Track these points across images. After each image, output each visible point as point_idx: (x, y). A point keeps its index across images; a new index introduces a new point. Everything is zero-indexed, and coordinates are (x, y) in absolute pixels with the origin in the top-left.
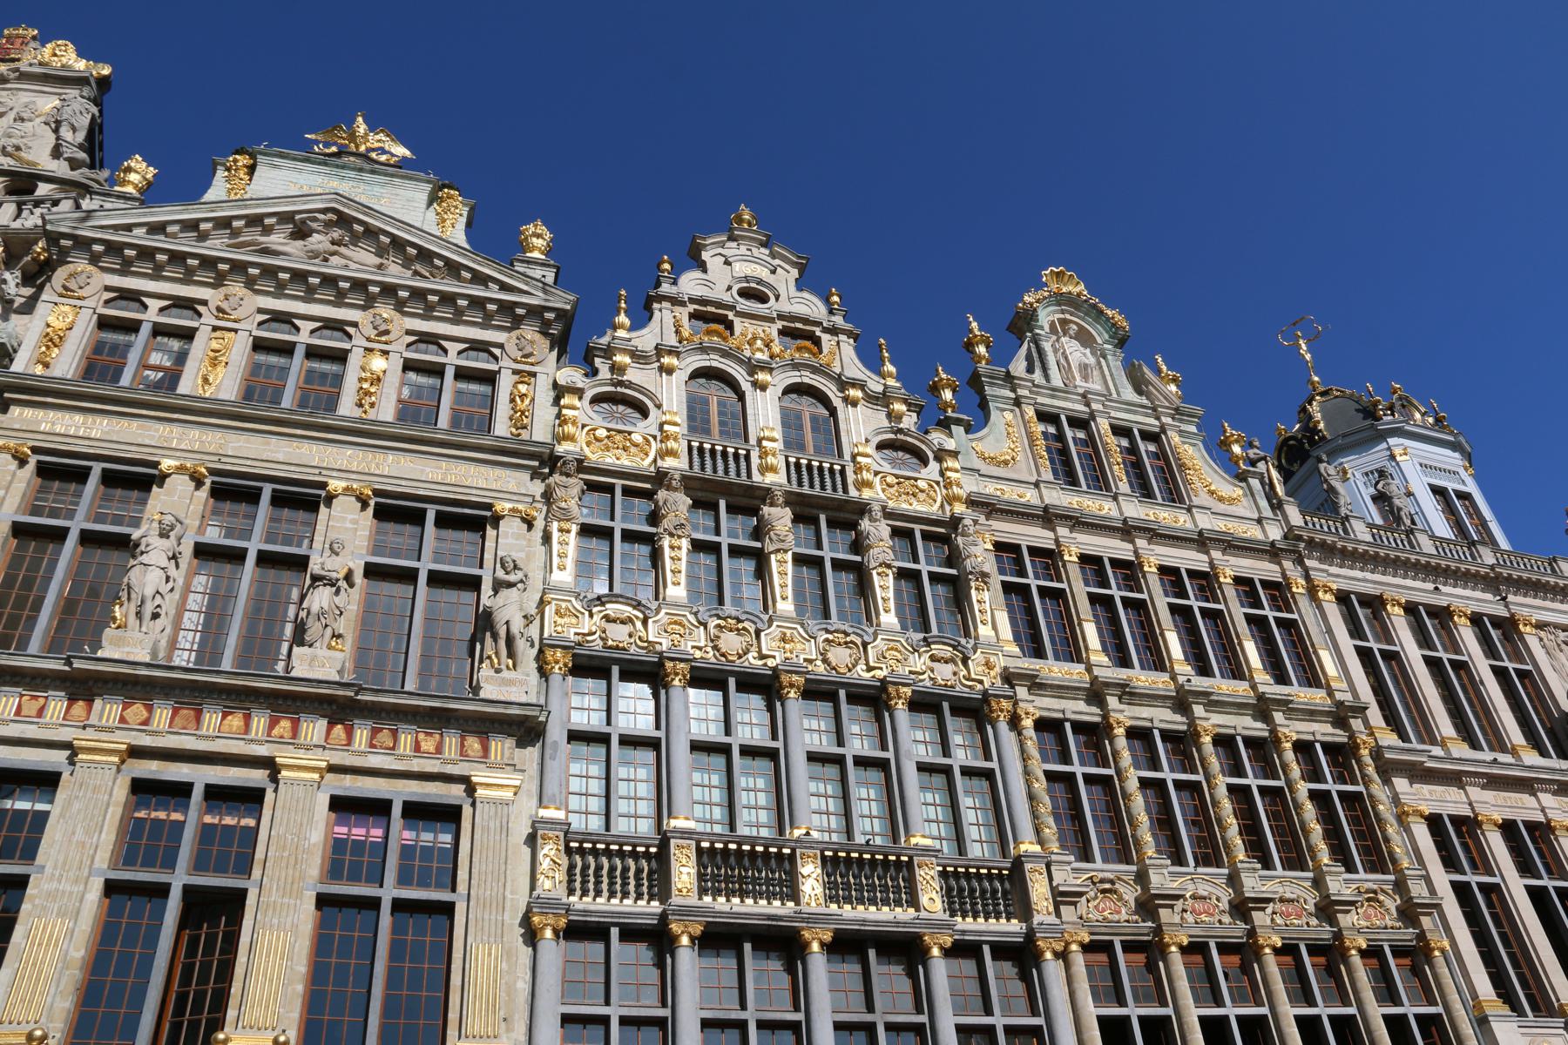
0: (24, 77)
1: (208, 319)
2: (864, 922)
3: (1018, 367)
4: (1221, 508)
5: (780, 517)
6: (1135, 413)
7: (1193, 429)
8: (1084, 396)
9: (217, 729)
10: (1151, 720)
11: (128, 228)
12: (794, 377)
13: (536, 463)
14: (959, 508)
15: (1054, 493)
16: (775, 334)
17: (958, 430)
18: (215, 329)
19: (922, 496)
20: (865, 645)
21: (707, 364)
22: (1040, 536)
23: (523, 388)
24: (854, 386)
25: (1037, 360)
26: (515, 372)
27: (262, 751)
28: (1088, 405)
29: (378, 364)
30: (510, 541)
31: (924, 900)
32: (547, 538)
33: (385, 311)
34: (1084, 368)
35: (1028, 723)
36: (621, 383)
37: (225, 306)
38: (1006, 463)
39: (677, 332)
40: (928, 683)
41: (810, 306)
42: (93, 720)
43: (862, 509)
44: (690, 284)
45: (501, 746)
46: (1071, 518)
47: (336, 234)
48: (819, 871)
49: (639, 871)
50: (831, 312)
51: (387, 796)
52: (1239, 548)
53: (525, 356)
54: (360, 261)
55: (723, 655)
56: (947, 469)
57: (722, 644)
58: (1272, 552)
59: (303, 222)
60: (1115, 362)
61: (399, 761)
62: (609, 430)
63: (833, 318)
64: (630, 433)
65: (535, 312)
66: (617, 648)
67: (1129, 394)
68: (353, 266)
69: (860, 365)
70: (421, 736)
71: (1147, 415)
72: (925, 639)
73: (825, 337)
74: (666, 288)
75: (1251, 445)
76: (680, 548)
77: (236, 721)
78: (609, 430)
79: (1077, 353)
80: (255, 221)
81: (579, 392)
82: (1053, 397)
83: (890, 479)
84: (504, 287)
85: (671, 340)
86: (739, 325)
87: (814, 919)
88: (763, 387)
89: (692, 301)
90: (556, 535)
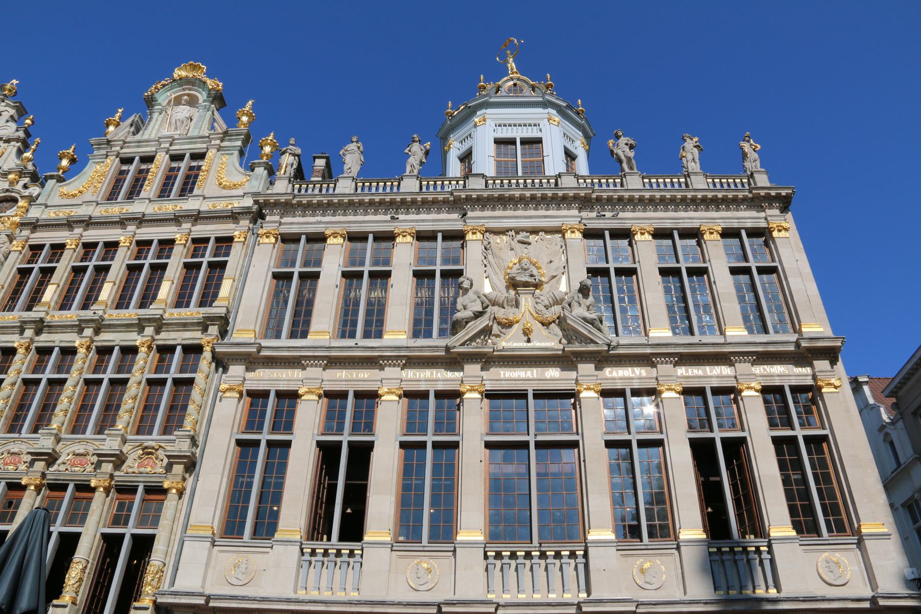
4: (226, 192)
6: (195, 143)
7: (239, 143)
38: (74, 196)
50: (17, 130)
52: (204, 218)
58: (234, 216)
71: (204, 142)
82: (138, 147)
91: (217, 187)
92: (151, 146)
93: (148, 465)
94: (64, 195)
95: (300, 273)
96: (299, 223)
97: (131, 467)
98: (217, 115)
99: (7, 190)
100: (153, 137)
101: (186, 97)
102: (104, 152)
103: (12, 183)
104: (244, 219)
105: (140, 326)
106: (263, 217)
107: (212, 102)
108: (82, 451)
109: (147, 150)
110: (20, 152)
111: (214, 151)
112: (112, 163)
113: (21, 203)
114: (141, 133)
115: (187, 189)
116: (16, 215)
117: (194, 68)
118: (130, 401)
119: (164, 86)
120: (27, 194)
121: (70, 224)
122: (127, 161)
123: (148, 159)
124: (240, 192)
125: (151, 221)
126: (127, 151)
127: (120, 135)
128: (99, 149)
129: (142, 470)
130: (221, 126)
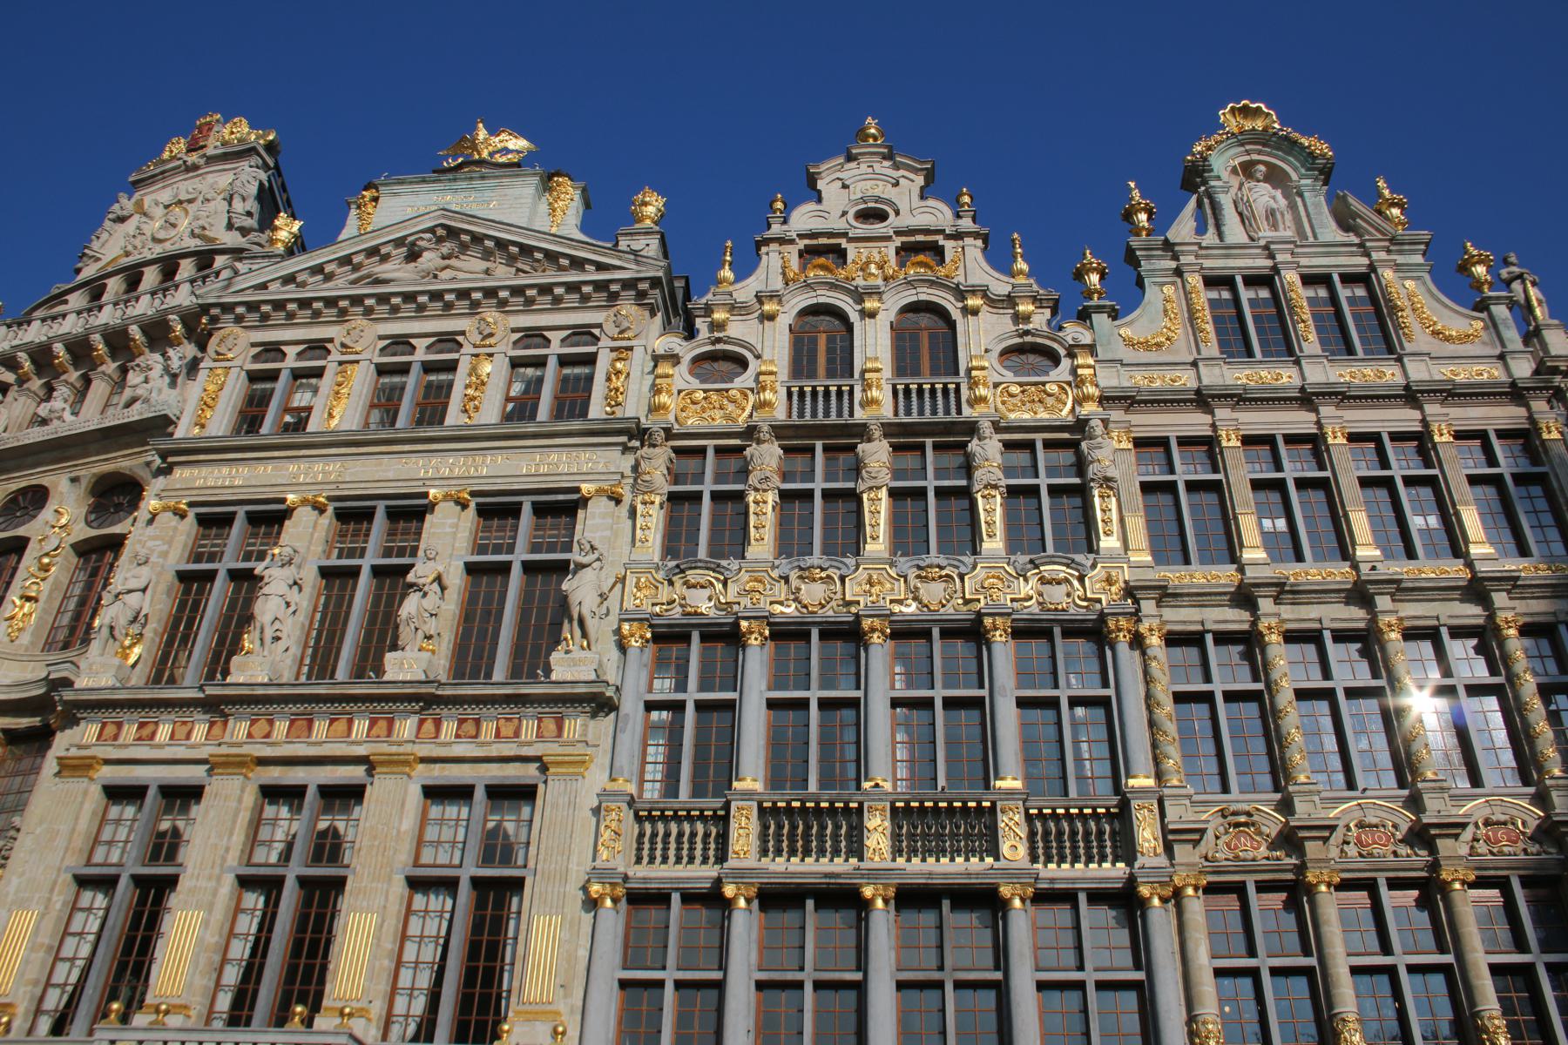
0: (211, 160)
1: (335, 356)
3: (1183, 229)
4: (1450, 349)
5: (877, 454)
6: (1337, 254)
8: (1266, 247)
9: (322, 736)
10: (1320, 621)
12: (909, 297)
13: (624, 439)
14: (1089, 409)
15: (1216, 370)
16: (892, 252)
17: (1100, 320)
18: (341, 363)
19: (1050, 401)
20: (962, 577)
21: (814, 301)
22: (1195, 422)
23: (619, 365)
24: (973, 292)
25: (1210, 215)
26: (613, 350)
27: (361, 751)
28: (1272, 256)
29: (486, 368)
30: (597, 521)
31: (1005, 848)
32: (633, 513)
33: (491, 315)
34: (1271, 214)
35: (1154, 641)
36: (719, 340)
37: (347, 341)
38: (1159, 345)
39: (784, 274)
40: (1036, 609)
41: (937, 214)
42: (227, 739)
43: (971, 428)
44: (804, 218)
45: (576, 725)
46: (1232, 396)
47: (446, 248)
48: (887, 824)
49: (707, 835)
50: (958, 216)
51: (470, 782)
52: (1459, 395)
53: (621, 332)
55: (805, 607)
56: (1078, 366)
57: (803, 596)
59: (413, 244)
60: (1316, 200)
61: (475, 747)
62: (705, 391)
63: (960, 222)
64: (727, 390)
65: (628, 284)
66: (696, 613)
67: (1330, 231)
68: (461, 275)
69: (988, 268)
70: (502, 722)
71: (1352, 254)
72: (1031, 561)
73: (949, 245)
74: (776, 229)
75: (1506, 263)
76: (765, 502)
77: (341, 726)
78: (705, 391)
79: (1264, 196)
80: (373, 252)
81: (674, 359)
82: (1227, 256)
83: (1015, 389)
84: (600, 267)
85: (777, 284)
86: (852, 251)
88: (872, 315)
89: (801, 236)
90: (640, 507)
91: (1431, 339)
94: (1130, 343)
101: (1262, 168)
102: (1173, 264)
103: (1027, 318)
108: (1503, 818)
125: (1360, 397)
126: (1216, 264)
128: (1149, 258)
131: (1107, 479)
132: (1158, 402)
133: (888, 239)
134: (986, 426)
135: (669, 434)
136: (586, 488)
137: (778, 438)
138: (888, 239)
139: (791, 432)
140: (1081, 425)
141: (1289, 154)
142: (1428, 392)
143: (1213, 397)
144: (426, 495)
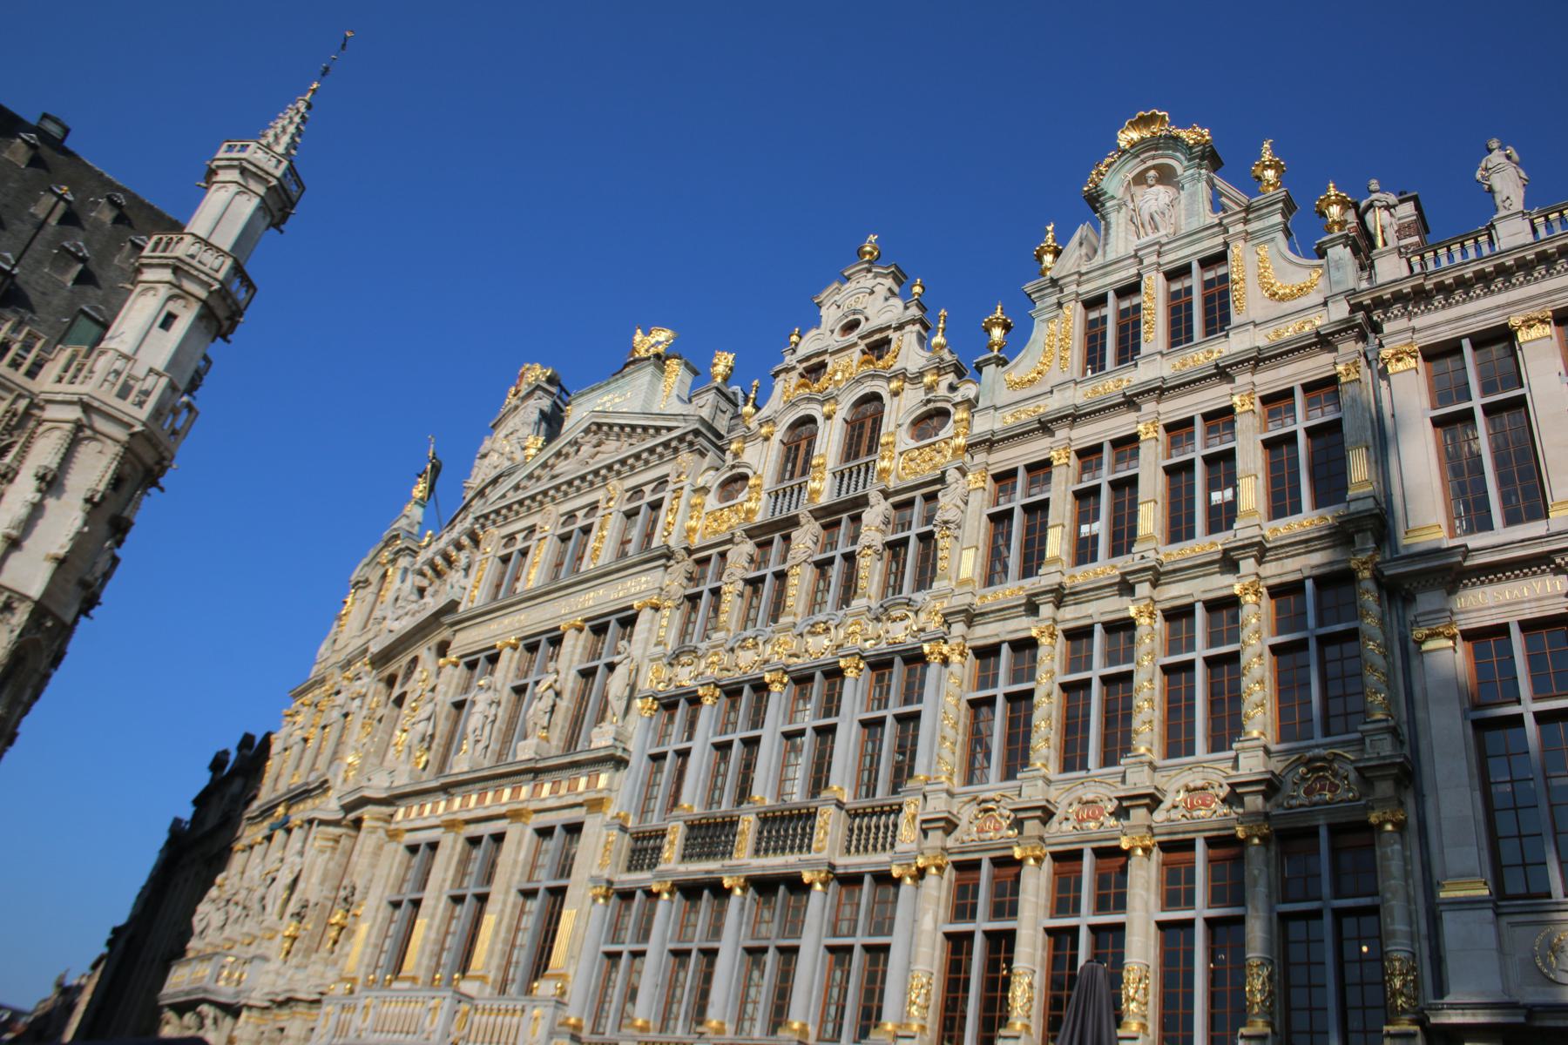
2: (763, 867)
7: (1278, 218)
8: (1136, 256)
11: (504, 496)
13: (663, 561)
40: (883, 645)
41: (895, 310)
44: (809, 344)
46: (1066, 417)
50: (906, 308)
52: (1269, 358)
54: (614, 450)
58: (1324, 341)
65: (681, 439)
71: (1215, 235)
82: (1105, 275)
84: (669, 429)
87: (731, 870)
91: (1272, 303)
92: (1130, 266)
93: (1322, 788)
94: (1013, 386)
95: (1483, 406)
96: (1449, 322)
97: (1293, 797)
98: (1221, 184)
99: (929, 401)
100: (1122, 253)
101: (1152, 173)
102: (1054, 299)
103: (930, 388)
104: (1344, 340)
105: (1228, 562)
106: (1377, 328)
107: (1200, 166)
108: (1199, 783)
109: (1125, 274)
110: (922, 341)
111: (1241, 244)
112: (1074, 315)
113: (959, 414)
114: (1100, 252)
115: (1218, 318)
116: (957, 435)
117: (1146, 122)
118: (1257, 687)
119: (1109, 166)
120: (958, 399)
121: (1045, 427)
122: (1096, 302)
123: (1130, 289)
124: (1315, 298)
126: (1090, 288)
127: (1069, 265)
129: (1316, 798)
130: (1234, 196)
131: (946, 522)
132: (1012, 437)
133: (855, 345)
134: (874, 495)
135: (689, 551)
136: (636, 604)
137: (751, 537)
138: (855, 345)
139: (757, 532)
140: (941, 479)
141: (1176, 150)
142: (1236, 364)
143: (1051, 421)
144: (558, 628)
